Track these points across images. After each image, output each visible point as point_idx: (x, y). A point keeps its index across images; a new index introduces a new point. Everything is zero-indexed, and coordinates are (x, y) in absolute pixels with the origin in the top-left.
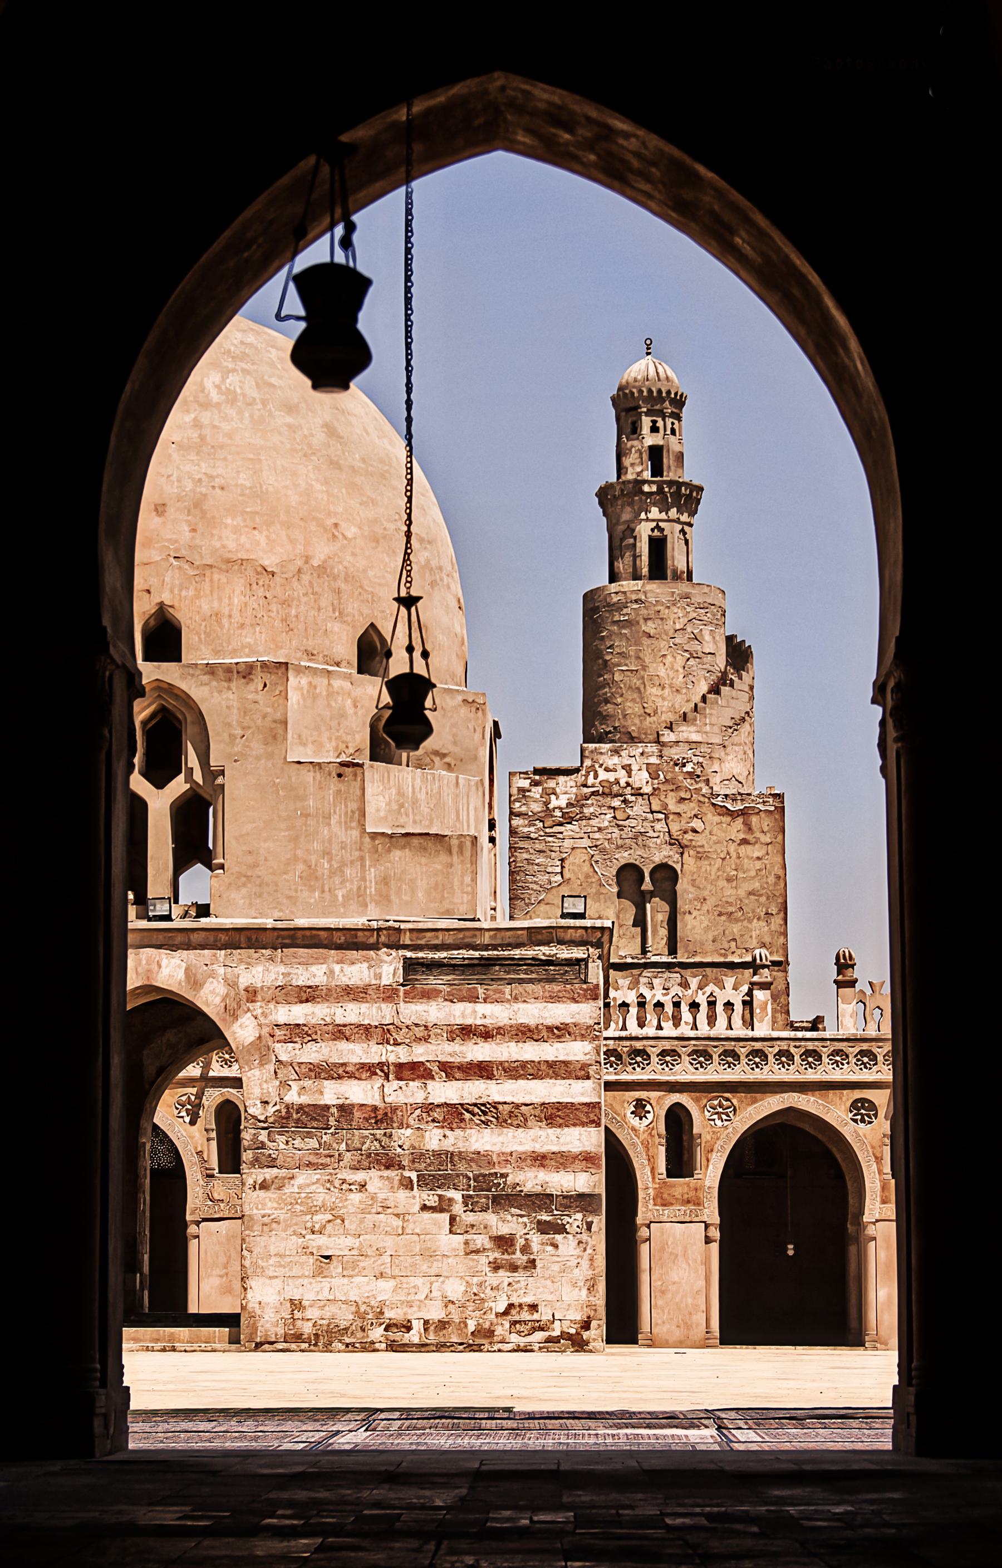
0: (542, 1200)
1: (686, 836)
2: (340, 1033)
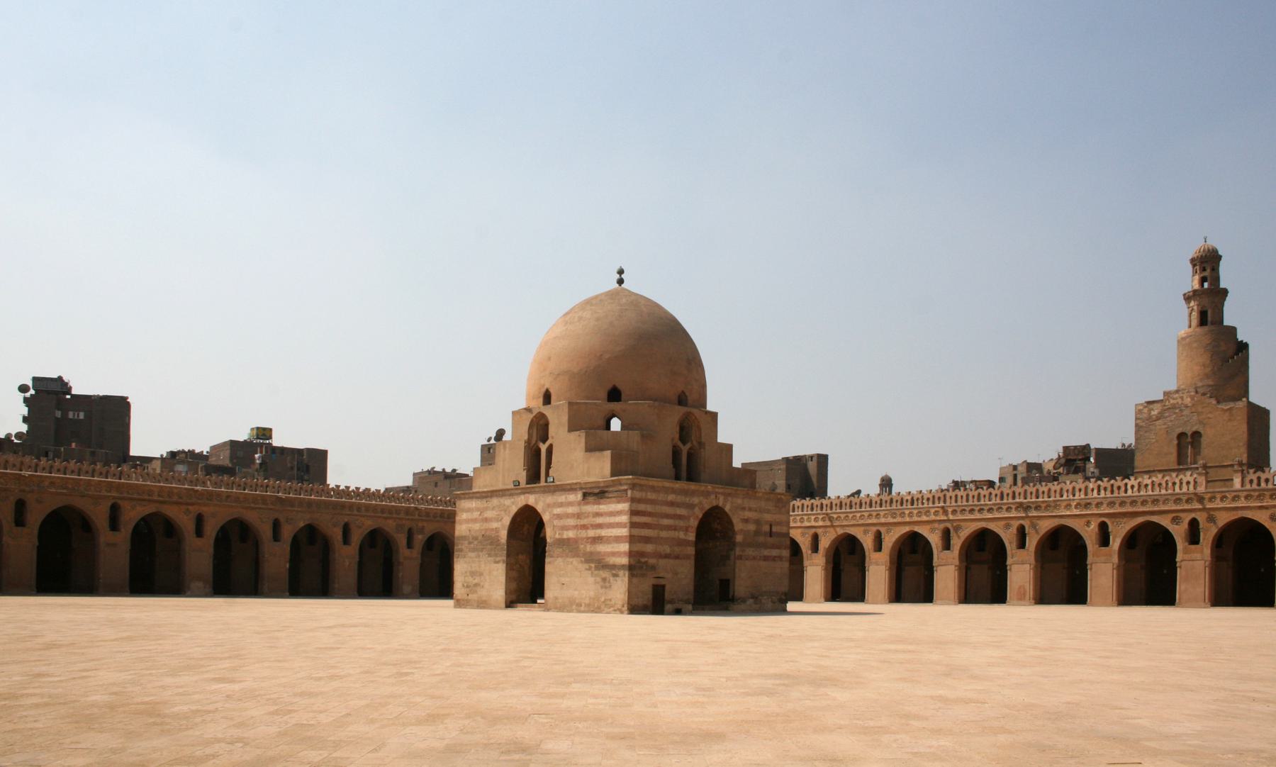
0: (613, 567)
2: (568, 516)
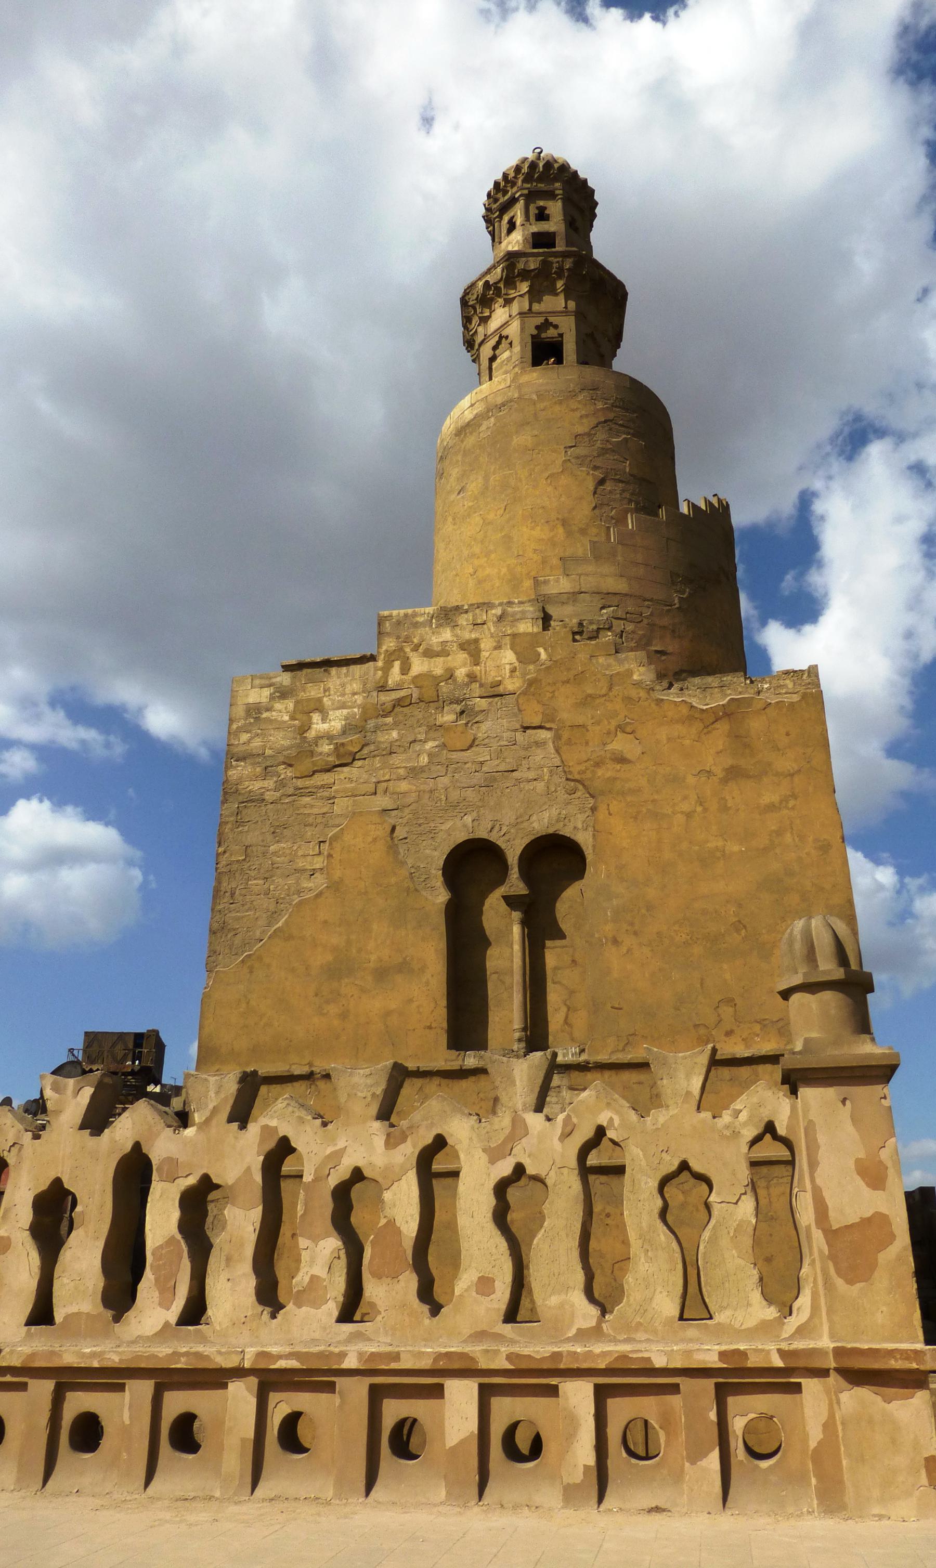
1: (600, 772)
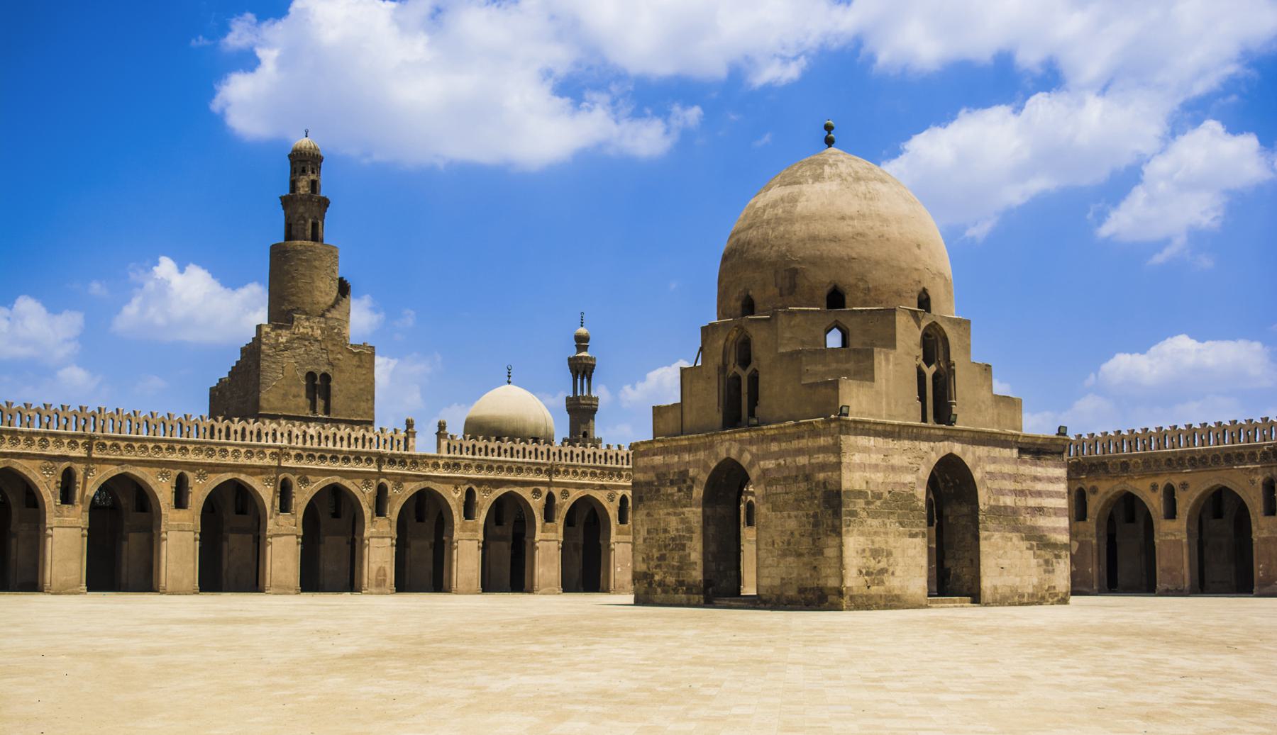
0: (1054, 546)
2: (1004, 476)
